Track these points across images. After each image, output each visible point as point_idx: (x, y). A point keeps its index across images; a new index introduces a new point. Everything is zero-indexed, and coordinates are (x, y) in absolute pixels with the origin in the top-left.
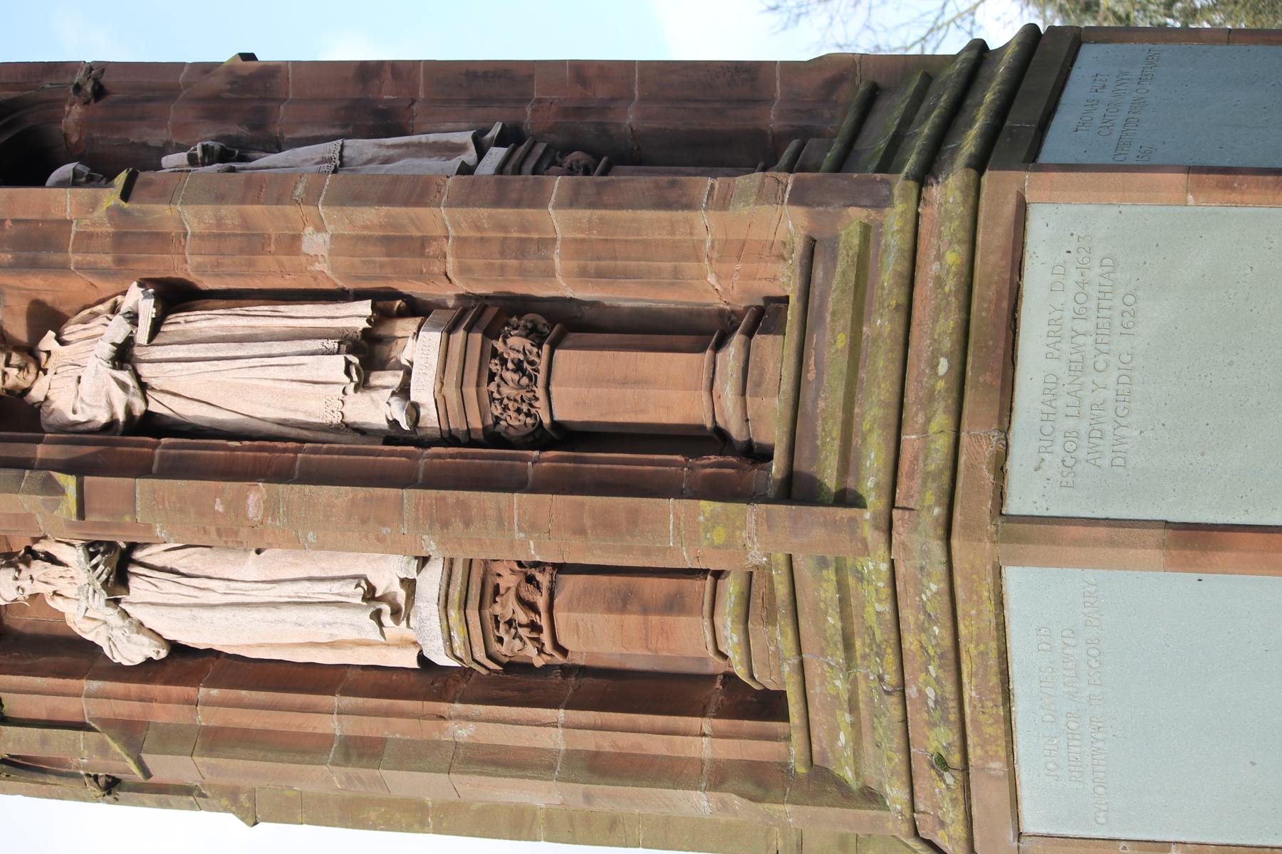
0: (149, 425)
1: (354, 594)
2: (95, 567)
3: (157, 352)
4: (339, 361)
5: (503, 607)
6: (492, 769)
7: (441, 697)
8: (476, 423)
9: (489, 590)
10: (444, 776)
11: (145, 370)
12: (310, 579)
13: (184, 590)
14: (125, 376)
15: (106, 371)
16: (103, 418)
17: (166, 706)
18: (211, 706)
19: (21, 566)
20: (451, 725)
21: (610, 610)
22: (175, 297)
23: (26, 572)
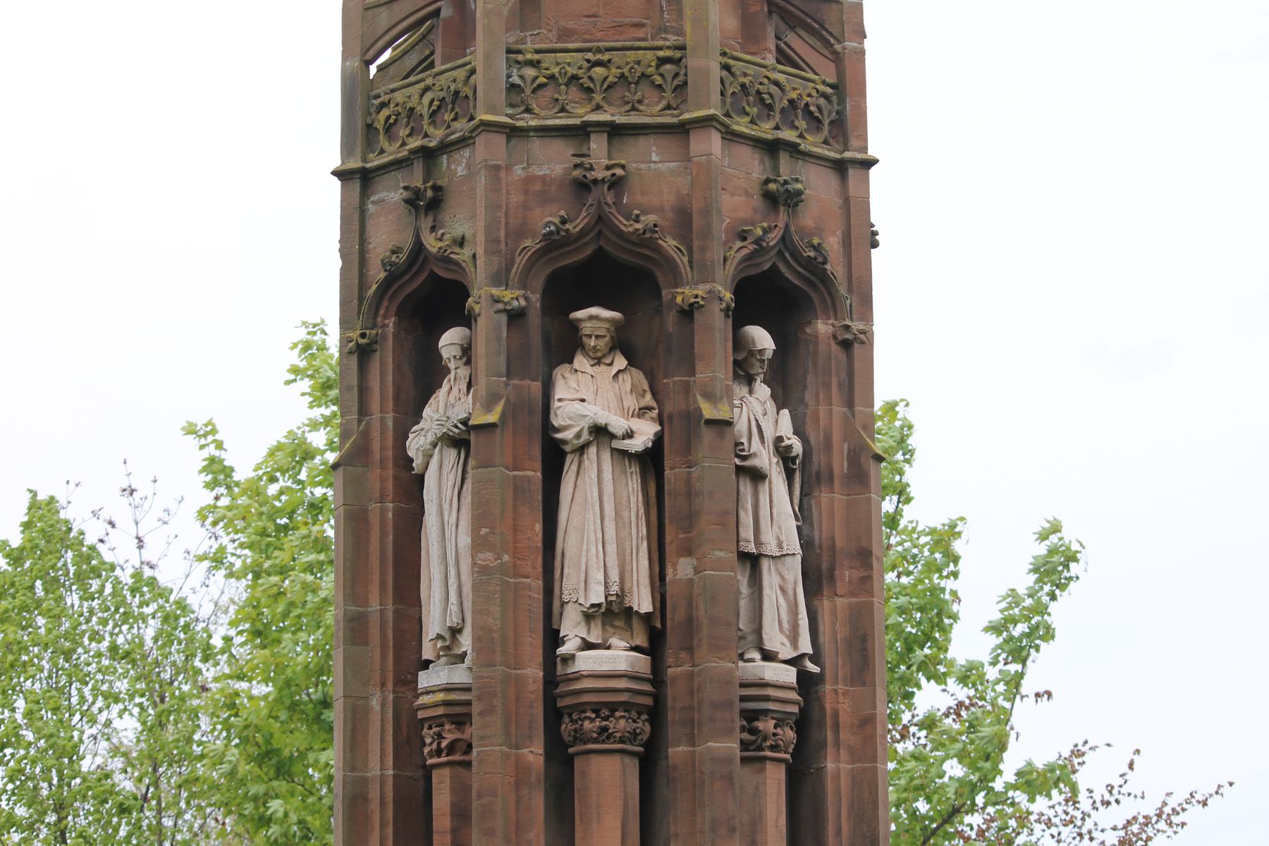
0: (554, 457)
1: (454, 620)
2: (456, 427)
3: (606, 456)
4: (602, 600)
5: (449, 731)
6: (349, 727)
7: (397, 683)
8: (561, 703)
9: (460, 719)
10: (341, 694)
11: (592, 450)
12: (460, 586)
13: (449, 492)
14: (585, 436)
15: (585, 424)
16: (556, 422)
17: (380, 478)
18: (385, 512)
19: (464, 359)
20: (378, 694)
21: (453, 805)
22: (651, 462)
23: (460, 363)
